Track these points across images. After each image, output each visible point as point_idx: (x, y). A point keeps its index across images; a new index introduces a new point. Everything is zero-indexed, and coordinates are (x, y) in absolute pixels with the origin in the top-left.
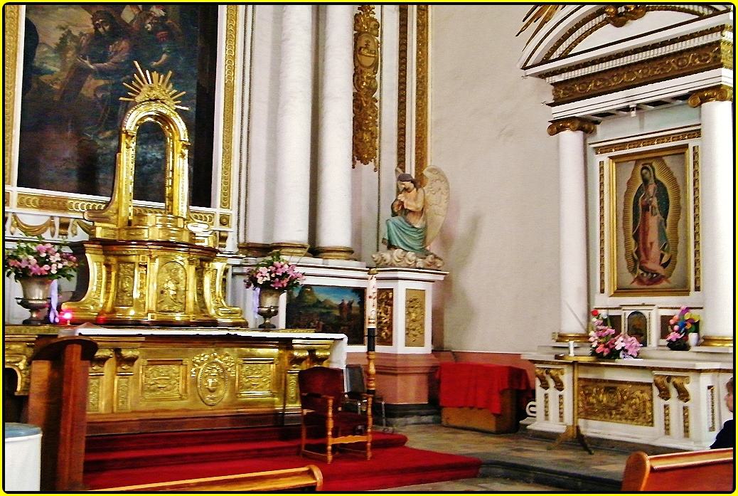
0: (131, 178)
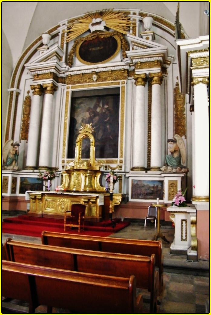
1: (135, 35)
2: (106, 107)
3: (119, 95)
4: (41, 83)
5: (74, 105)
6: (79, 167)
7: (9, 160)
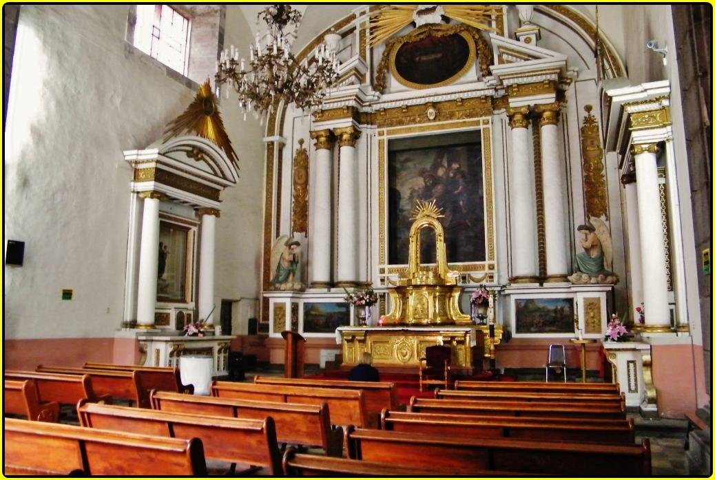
0: (438, 251)
1: (502, 35)
2: (455, 166)
3: (480, 143)
4: (331, 128)
5: (394, 164)
7: (282, 272)
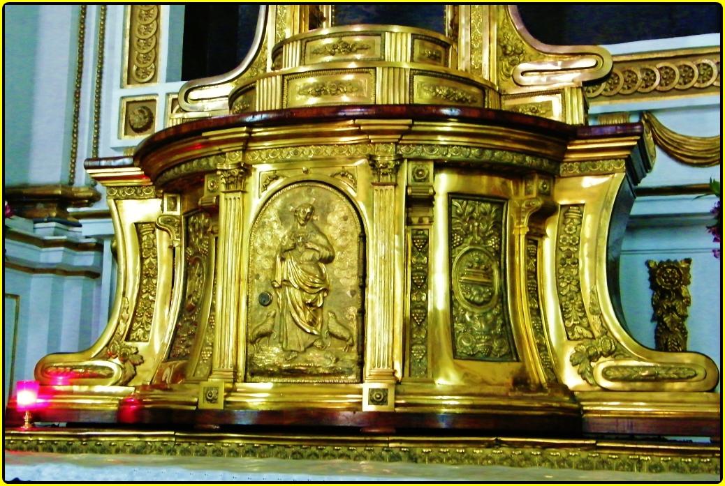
6: (319, 92)
